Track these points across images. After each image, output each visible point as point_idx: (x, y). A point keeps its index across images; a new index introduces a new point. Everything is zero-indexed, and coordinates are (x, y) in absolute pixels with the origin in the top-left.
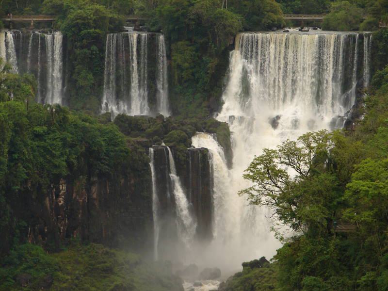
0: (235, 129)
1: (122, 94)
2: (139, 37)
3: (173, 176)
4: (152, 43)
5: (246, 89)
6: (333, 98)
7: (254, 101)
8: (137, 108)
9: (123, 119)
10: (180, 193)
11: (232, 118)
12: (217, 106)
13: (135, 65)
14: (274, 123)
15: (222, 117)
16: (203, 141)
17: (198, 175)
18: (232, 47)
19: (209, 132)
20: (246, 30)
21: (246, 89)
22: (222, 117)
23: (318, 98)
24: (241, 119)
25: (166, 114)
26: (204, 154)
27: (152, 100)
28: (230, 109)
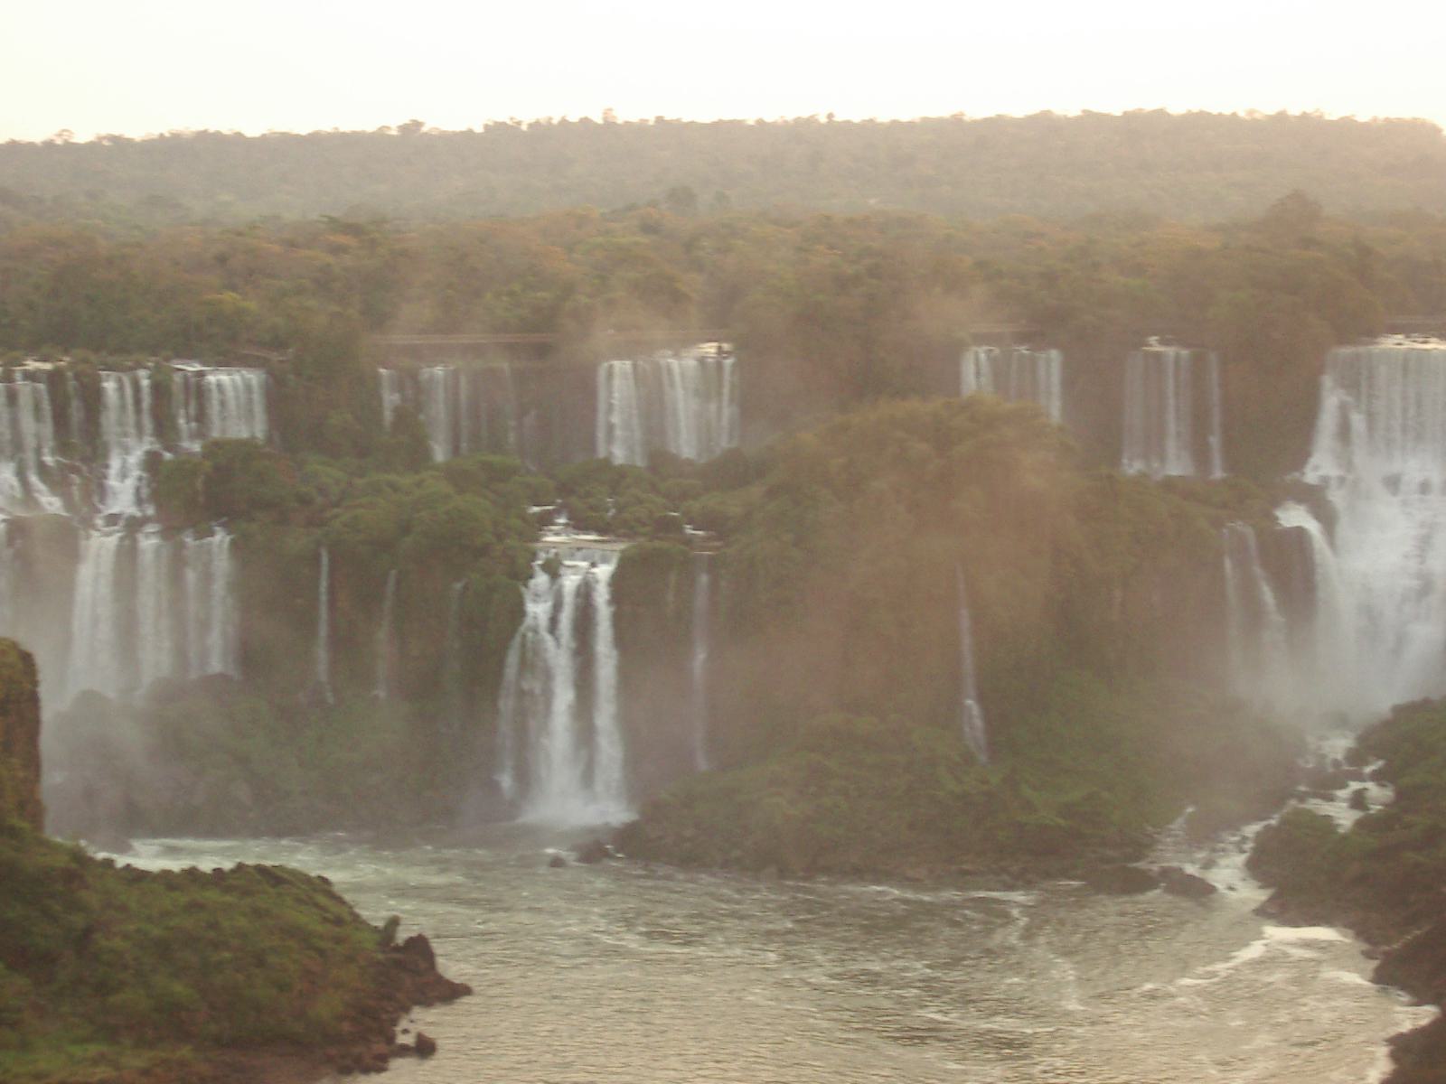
0: (1337, 497)
1: (1153, 445)
3: (1257, 570)
4: (1198, 362)
5: (1344, 432)
7: (1360, 457)
8: (1177, 466)
9: (1169, 485)
10: (1268, 595)
11: (1325, 479)
12: (1301, 456)
13: (1171, 402)
15: (1311, 477)
16: (1294, 516)
17: (1292, 566)
18: (1320, 371)
19: (1300, 501)
20: (1342, 341)
21: (1344, 432)
22: (1311, 477)
24: (1342, 480)
25: (1218, 474)
26: (1300, 532)
27: (1200, 455)
28: (1321, 466)
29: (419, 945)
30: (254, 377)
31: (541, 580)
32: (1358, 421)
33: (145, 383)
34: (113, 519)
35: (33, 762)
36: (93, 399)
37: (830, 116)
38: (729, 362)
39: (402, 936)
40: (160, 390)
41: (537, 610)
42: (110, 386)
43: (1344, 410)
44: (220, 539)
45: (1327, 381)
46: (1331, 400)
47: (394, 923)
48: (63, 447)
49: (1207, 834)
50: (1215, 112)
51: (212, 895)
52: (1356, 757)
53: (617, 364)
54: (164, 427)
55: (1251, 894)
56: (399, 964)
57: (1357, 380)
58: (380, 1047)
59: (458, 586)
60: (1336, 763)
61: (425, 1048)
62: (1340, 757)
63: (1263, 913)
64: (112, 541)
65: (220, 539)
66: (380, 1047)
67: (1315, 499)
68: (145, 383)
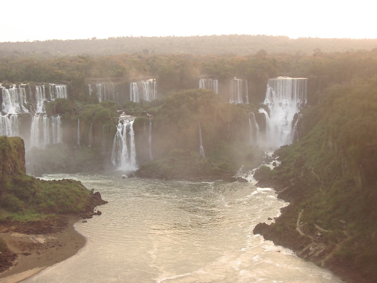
0: (270, 107)
2: (240, 80)
5: (271, 95)
6: (297, 97)
7: (274, 99)
9: (238, 105)
10: (257, 125)
12: (263, 99)
14: (280, 104)
15: (265, 103)
16: (262, 111)
17: (262, 121)
18: (267, 83)
21: (271, 95)
22: (265, 103)
23: (292, 97)
26: (263, 114)
27: (244, 99)
28: (267, 101)
29: (98, 194)
30: (65, 86)
31: (120, 124)
32: (274, 92)
33: (44, 88)
34: (38, 114)
35: (24, 160)
36: (34, 90)
37: (174, 36)
38: (155, 83)
39: (95, 192)
40: (47, 89)
41: (119, 130)
42: (37, 88)
43: (271, 90)
44: (59, 117)
45: (268, 85)
46: (269, 89)
47: (93, 190)
48: (28, 100)
49: (246, 171)
50: (268, 35)
51: (58, 185)
52: (274, 156)
53: (134, 83)
54: (48, 96)
55: (255, 182)
56: (94, 198)
57: (274, 85)
58: (91, 213)
59: (104, 125)
60: (270, 157)
61: (99, 213)
62: (271, 156)
63: (257, 185)
64: (38, 118)
65: (59, 117)
66: (91, 213)
67: (266, 108)
68: (44, 88)
